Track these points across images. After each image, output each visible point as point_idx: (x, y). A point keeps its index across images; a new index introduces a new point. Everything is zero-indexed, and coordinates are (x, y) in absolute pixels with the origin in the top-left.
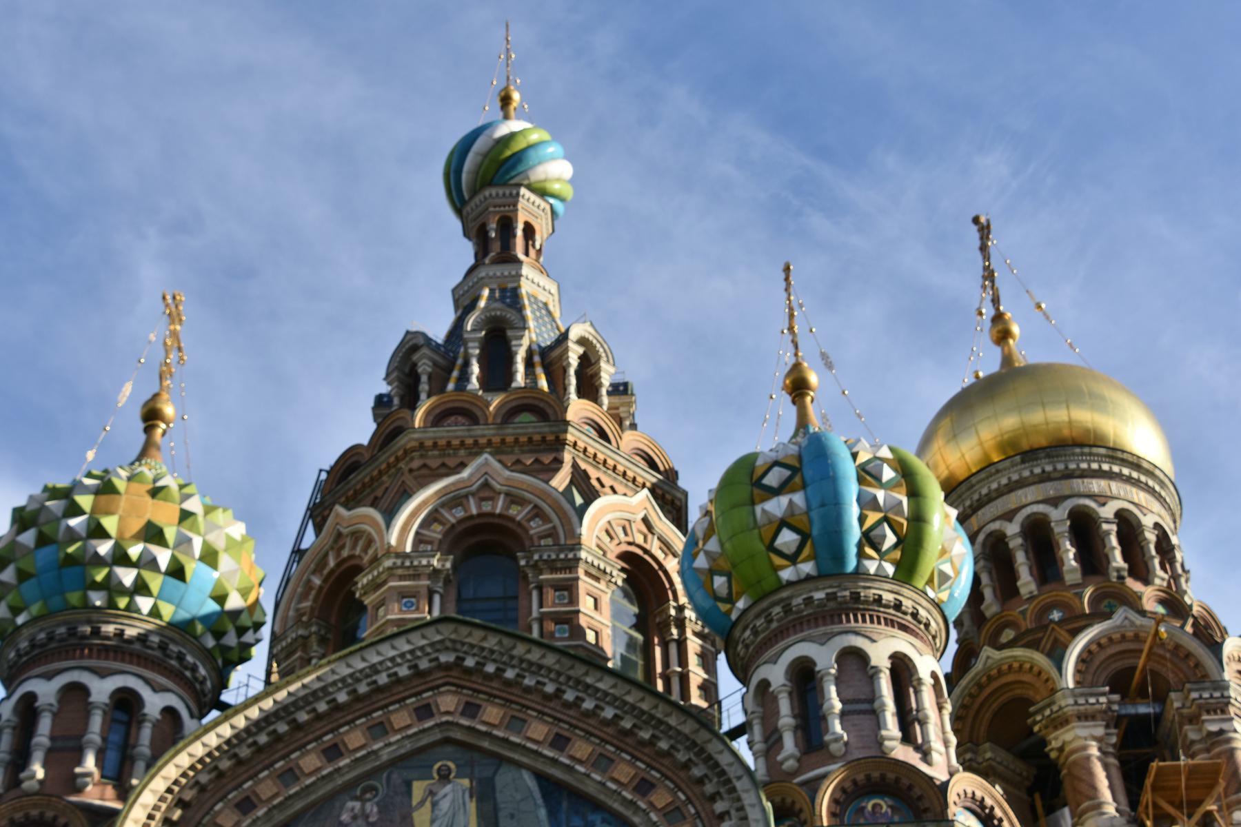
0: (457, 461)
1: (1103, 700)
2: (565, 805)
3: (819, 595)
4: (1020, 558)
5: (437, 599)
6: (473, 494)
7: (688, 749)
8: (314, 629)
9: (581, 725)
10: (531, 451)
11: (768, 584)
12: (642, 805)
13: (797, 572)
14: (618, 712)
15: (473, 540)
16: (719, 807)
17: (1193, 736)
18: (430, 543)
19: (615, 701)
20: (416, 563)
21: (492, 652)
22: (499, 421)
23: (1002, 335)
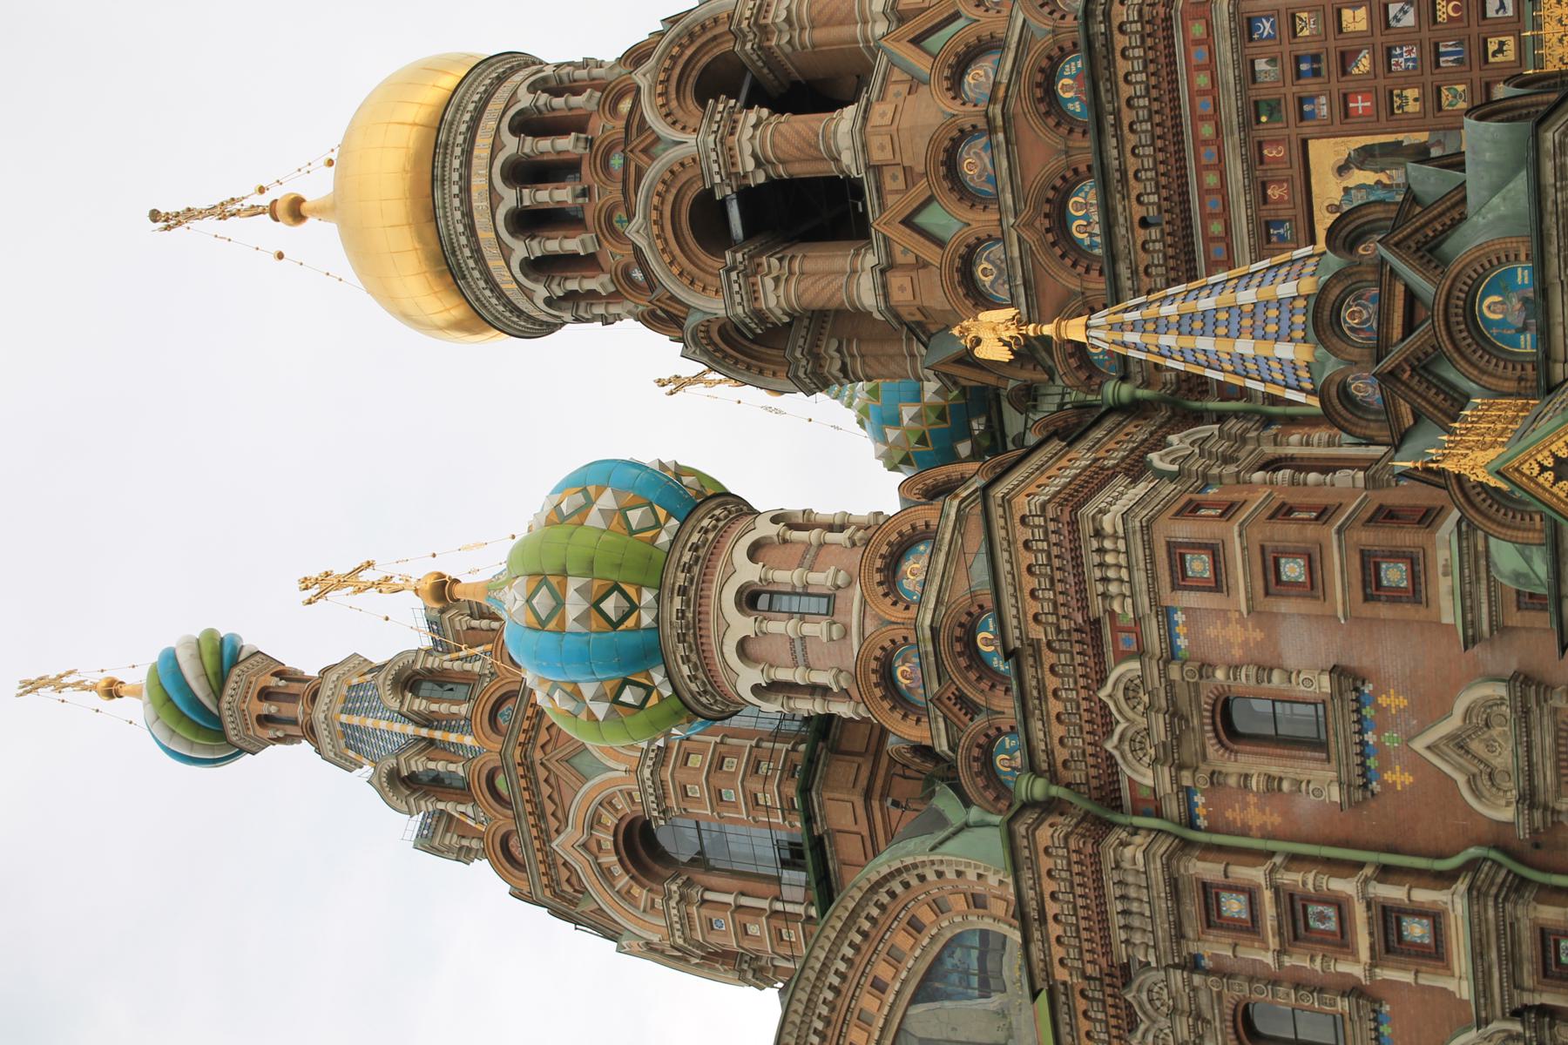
0: (562, 869)
1: (734, 275)
2: (937, 985)
3: (685, 670)
4: (572, 285)
5: (709, 896)
6: (596, 858)
7: (877, 893)
8: (745, 966)
9: (861, 969)
10: (537, 783)
11: (676, 703)
12: (934, 931)
13: (661, 683)
14: (847, 942)
15: (643, 853)
16: (931, 876)
17: (761, 178)
18: (653, 901)
19: (836, 944)
20: (676, 919)
21: (798, 1037)
22: (509, 812)
23: (296, 211)
